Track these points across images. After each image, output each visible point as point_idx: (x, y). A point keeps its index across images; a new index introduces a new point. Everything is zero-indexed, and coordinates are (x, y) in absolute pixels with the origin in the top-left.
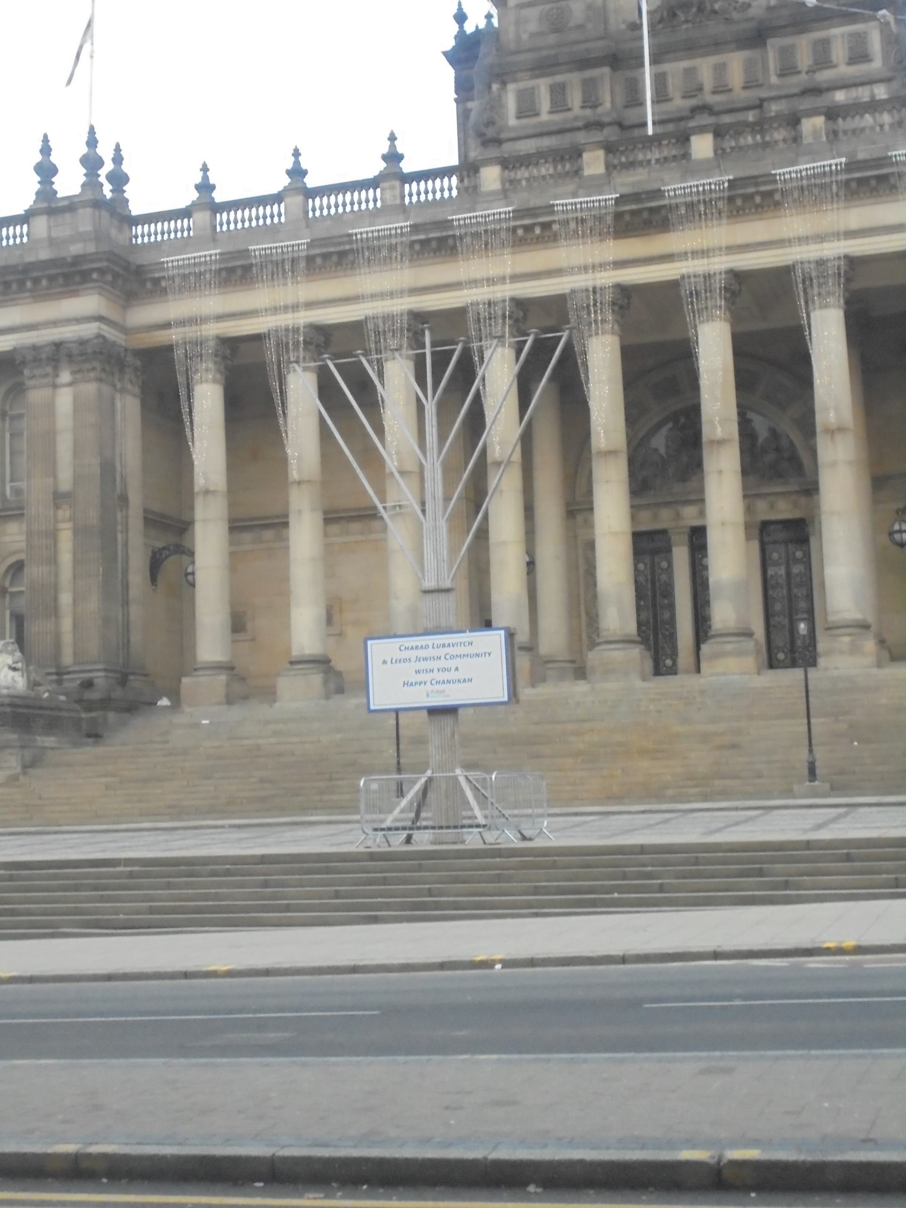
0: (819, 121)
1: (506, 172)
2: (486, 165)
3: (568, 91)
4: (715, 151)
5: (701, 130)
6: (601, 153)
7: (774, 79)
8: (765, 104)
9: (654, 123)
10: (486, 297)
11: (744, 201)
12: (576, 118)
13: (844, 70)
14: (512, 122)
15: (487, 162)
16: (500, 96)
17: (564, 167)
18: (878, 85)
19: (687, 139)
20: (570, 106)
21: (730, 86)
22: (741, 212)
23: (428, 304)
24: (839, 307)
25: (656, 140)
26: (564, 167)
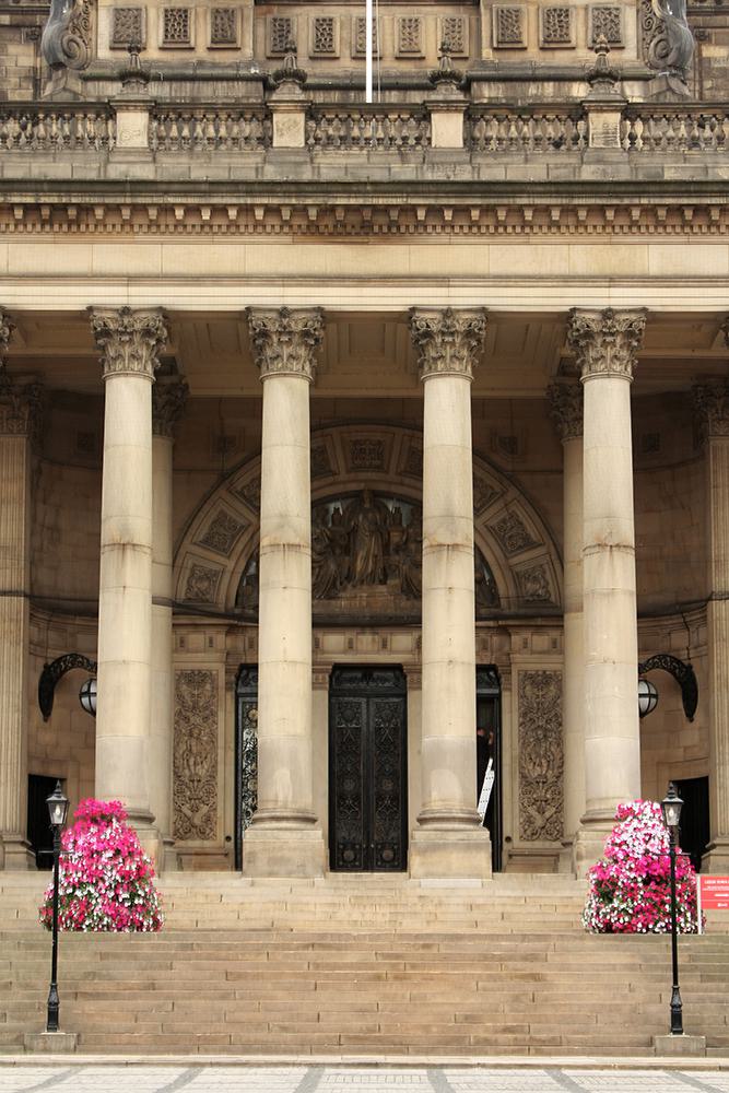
0: (614, 118)
1: (155, 124)
2: (127, 109)
3: (191, 22)
4: (465, 140)
5: (449, 107)
6: (301, 117)
7: (487, 54)
8: (475, 85)
9: (375, 88)
10: (603, 304)
11: (694, 215)
12: (201, 64)
13: (534, 56)
14: (104, 53)
15: (128, 105)
16: (86, 12)
17: (180, 131)
18: (630, 83)
19: (427, 117)
20: (192, 44)
21: (423, 54)
22: (501, 230)
23: (29, 300)
24: (625, 378)
25: (380, 111)
26: (180, 131)
